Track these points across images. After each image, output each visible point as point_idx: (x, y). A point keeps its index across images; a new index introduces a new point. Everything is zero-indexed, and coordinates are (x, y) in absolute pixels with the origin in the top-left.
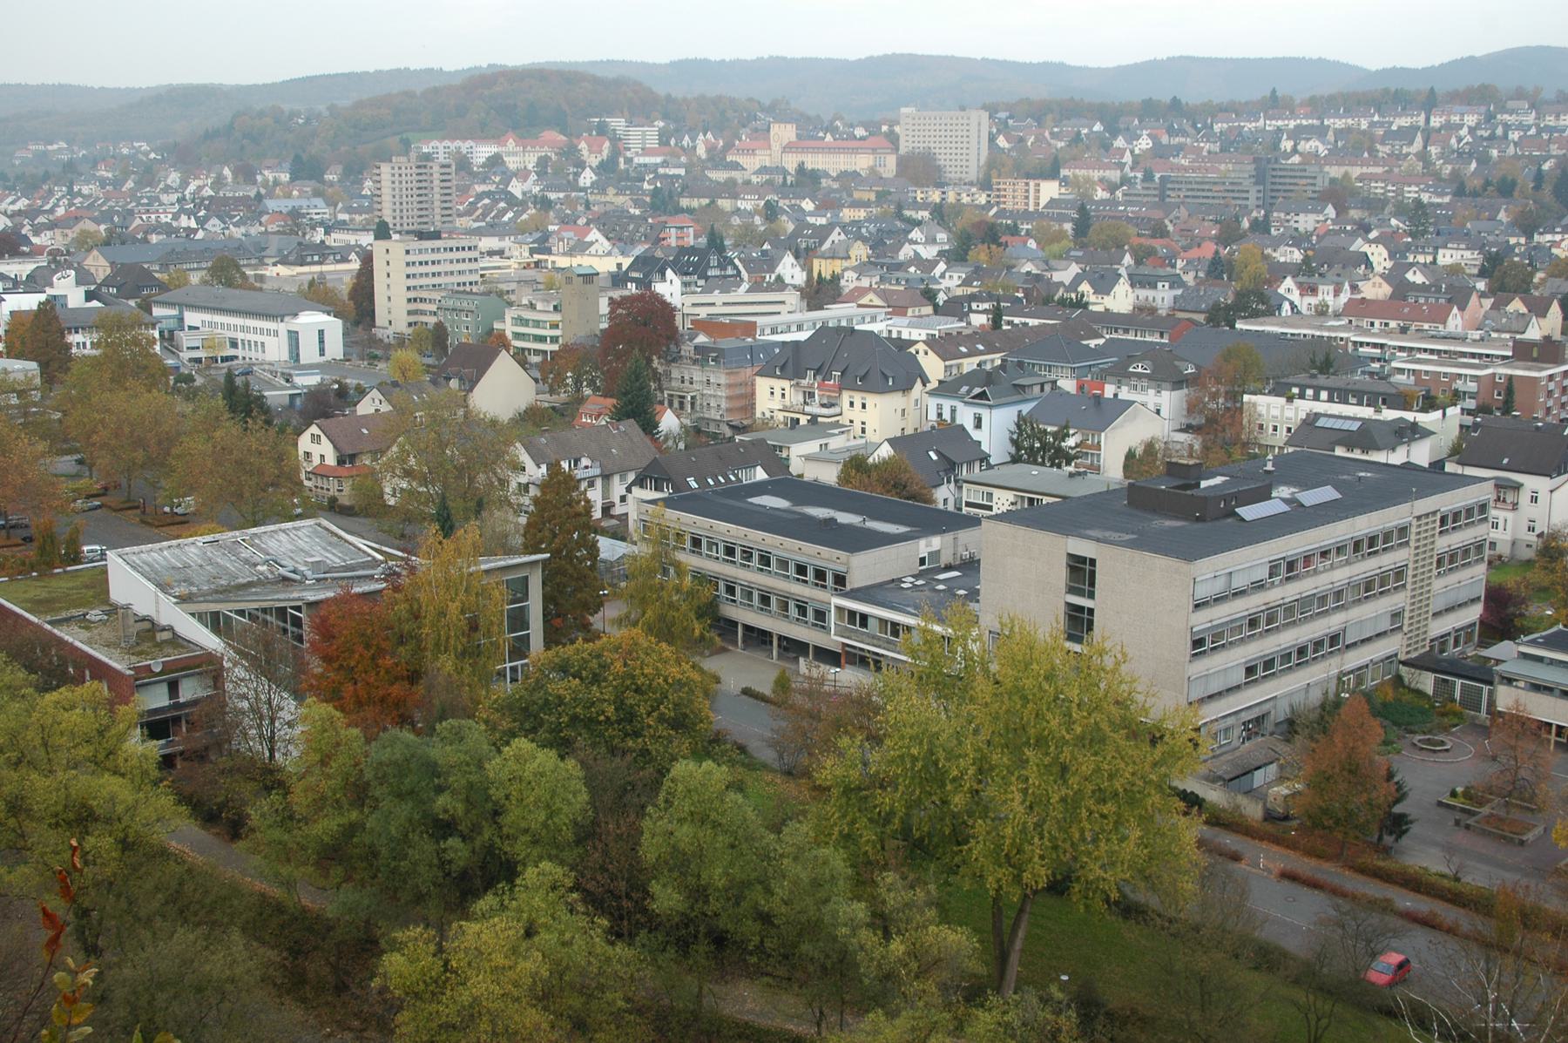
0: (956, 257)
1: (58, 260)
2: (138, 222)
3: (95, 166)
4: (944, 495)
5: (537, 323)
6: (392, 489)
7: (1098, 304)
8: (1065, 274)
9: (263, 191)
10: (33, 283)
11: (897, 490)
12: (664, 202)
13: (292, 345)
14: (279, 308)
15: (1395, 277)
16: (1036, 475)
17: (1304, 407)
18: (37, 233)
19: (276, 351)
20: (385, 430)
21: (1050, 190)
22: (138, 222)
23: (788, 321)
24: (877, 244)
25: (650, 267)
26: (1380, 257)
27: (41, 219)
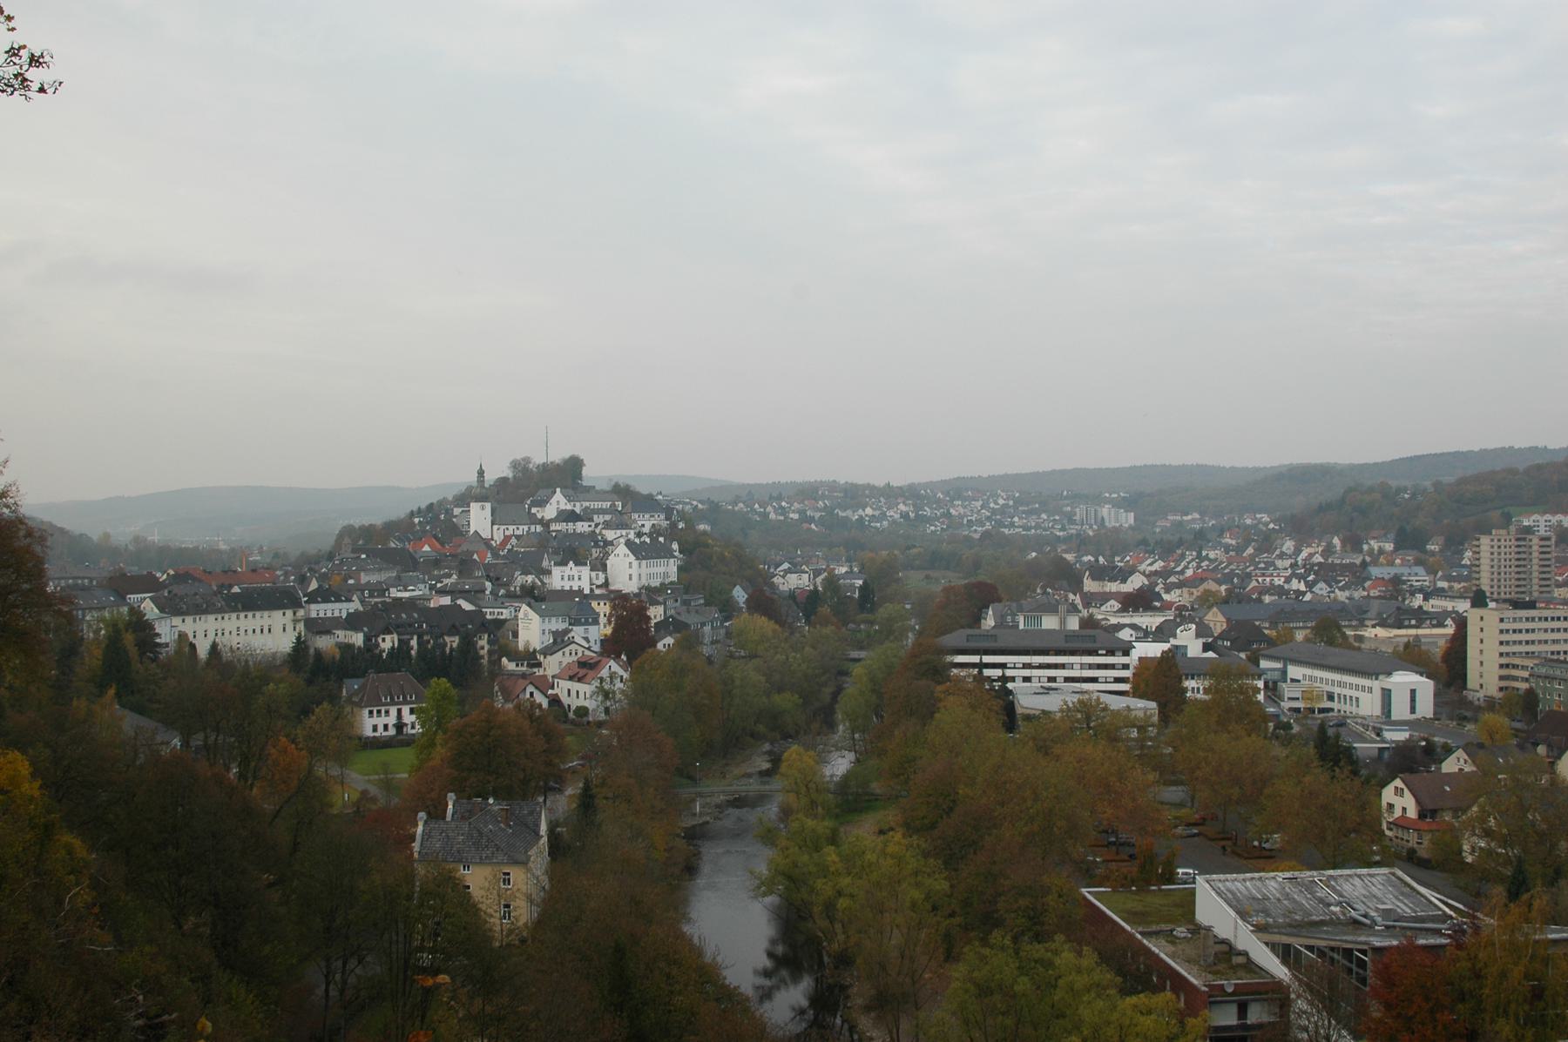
1: (1184, 615)
2: (1254, 584)
3: (1221, 535)
6: (1471, 847)
9: (1368, 559)
10: (1161, 634)
14: (1375, 666)
18: (1168, 591)
19: (1369, 706)
22: (1254, 584)
27: (1173, 579)
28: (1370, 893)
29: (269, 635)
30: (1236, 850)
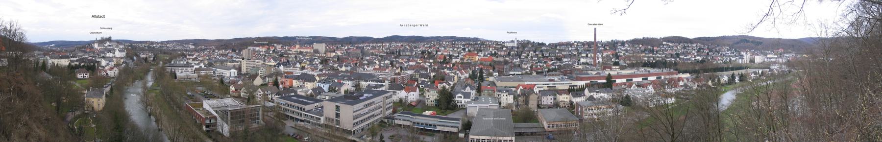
0: (321, 63)
4: (319, 97)
5: (262, 71)
6: (242, 94)
7: (340, 69)
8: (336, 65)
10: (198, 64)
11: (312, 98)
12: (281, 56)
13: (230, 74)
15: (379, 65)
16: (333, 94)
17: (368, 83)
20: (242, 86)
21: (334, 54)
23: (298, 72)
24: (311, 61)
25: (279, 65)
26: (377, 62)
28: (229, 102)
29: (65, 62)
30: (208, 97)
